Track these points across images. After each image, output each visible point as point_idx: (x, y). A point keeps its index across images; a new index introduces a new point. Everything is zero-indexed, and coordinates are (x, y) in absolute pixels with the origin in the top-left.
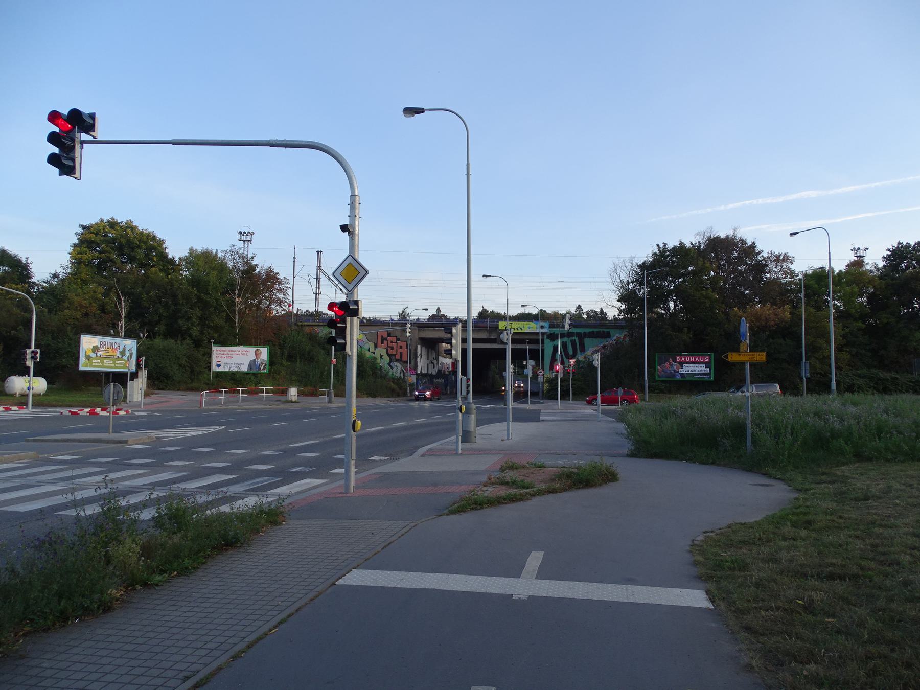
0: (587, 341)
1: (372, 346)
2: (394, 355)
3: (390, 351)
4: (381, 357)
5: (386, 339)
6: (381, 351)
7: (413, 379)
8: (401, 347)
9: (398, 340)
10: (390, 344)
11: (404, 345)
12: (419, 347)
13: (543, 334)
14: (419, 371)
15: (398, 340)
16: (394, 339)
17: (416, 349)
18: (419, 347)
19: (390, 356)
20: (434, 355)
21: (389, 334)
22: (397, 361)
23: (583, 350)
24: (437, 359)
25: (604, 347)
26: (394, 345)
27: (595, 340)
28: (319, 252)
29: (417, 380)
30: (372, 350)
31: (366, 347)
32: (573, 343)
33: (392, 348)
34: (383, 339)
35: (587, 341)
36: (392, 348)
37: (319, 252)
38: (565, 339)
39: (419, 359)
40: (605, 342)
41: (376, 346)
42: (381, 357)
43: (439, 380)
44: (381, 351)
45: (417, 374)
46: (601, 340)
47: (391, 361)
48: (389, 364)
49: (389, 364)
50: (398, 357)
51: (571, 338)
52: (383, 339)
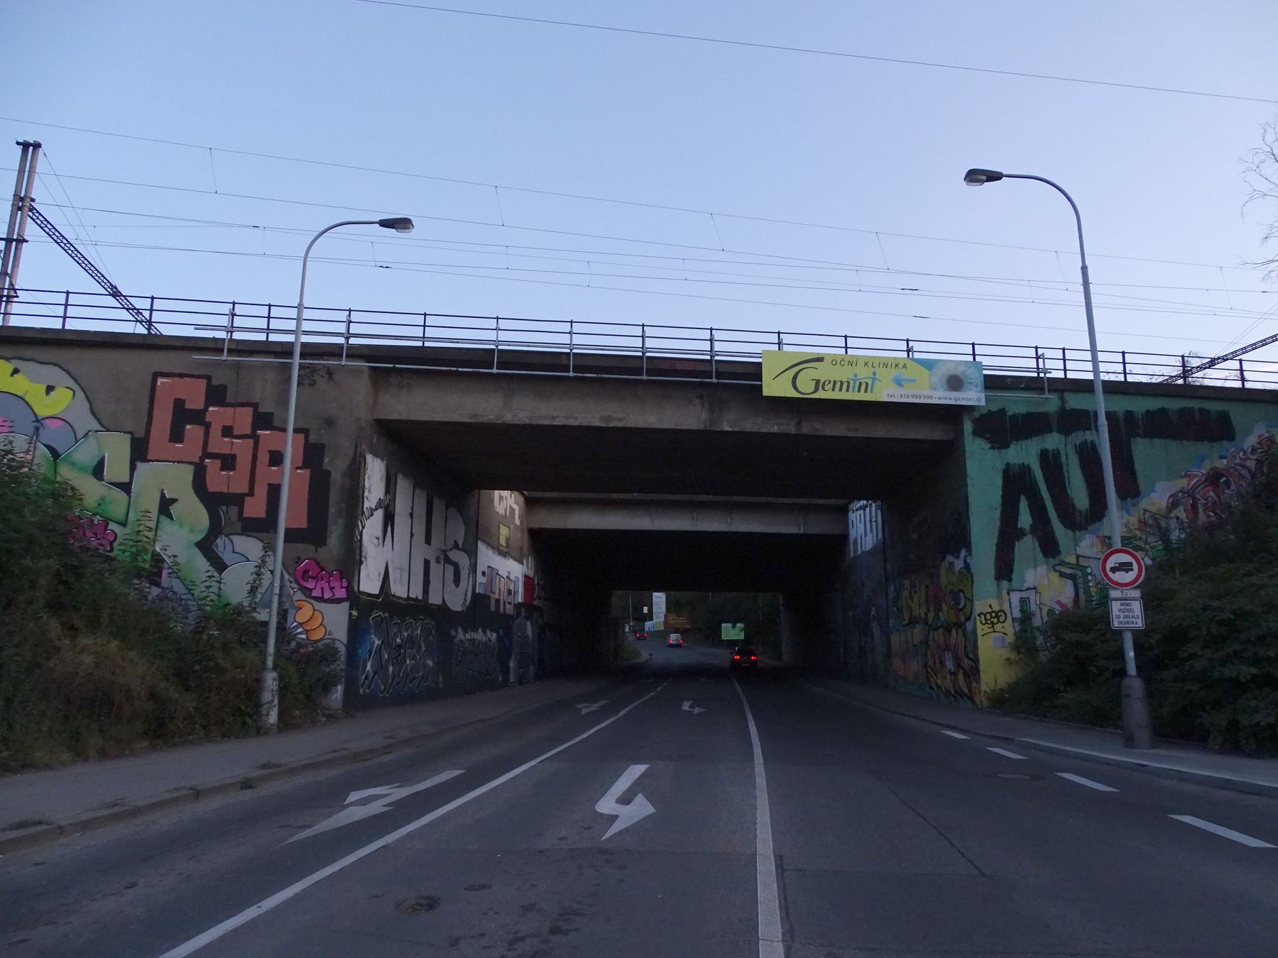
0: (1144, 451)
1: (116, 449)
2: (238, 500)
3: (217, 480)
4: (166, 505)
5: (198, 417)
6: (168, 476)
7: (333, 622)
8: (276, 458)
9: (263, 420)
10: (220, 444)
12: (375, 471)
13: (951, 415)
14: (369, 583)
15: (263, 420)
16: (243, 420)
17: (356, 473)
18: (375, 471)
19: (212, 501)
20: (459, 532)
21: (216, 395)
23: (1130, 489)
24: (473, 554)
25: (1214, 478)
26: (241, 448)
27: (1173, 445)
28: (29, 148)
29: (356, 630)
30: (117, 468)
31: (86, 454)
32: (1089, 457)
33: (228, 462)
34: (183, 416)
35: (1144, 451)
36: (228, 462)
37: (29, 148)
38: (1053, 441)
39: (372, 527)
40: (1215, 457)
41: (140, 451)
42: (166, 505)
43: (479, 636)
44: (168, 476)
45: (355, 598)
46: (1204, 447)
47: (216, 529)
48: (205, 546)
49: (205, 546)
51: (1079, 437)
52: (183, 416)
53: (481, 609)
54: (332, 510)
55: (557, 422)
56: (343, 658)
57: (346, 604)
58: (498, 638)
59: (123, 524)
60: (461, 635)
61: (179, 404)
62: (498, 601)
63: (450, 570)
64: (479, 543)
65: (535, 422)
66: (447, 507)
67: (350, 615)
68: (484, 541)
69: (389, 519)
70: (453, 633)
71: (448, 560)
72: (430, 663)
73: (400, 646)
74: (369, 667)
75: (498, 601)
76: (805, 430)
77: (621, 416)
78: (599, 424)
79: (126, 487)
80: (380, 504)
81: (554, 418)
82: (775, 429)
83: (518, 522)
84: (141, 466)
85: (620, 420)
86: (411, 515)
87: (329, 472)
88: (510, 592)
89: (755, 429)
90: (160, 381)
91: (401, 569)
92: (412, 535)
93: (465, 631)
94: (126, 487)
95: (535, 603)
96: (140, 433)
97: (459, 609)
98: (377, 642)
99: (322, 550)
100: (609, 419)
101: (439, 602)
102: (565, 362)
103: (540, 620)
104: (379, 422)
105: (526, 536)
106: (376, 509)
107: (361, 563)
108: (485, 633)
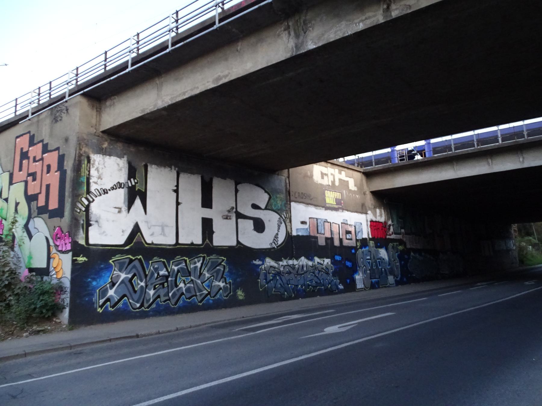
9: (45, 149)
11: (52, 158)
15: (45, 149)
22: (42, 211)
50: (41, 202)
53: (298, 245)
54: (67, 194)
55: (187, 96)
56: (69, 290)
57: (71, 254)
58: (334, 262)
59: (6, 220)
60: (269, 262)
61: (22, 149)
62: (330, 240)
63: (247, 226)
64: (293, 204)
65: (174, 101)
66: (237, 184)
67: (74, 261)
68: (295, 202)
69: (136, 194)
70: (257, 262)
71: (239, 216)
72: (222, 284)
73: (167, 277)
74: (111, 293)
75: (330, 240)
76: (395, 13)
77: (226, 72)
78: (211, 86)
79: (6, 200)
80: (120, 185)
81: (184, 93)
82: (361, 27)
83: (352, 186)
84: (11, 187)
85: (226, 76)
86: (176, 191)
87: (66, 170)
88: (348, 232)
89: (340, 35)
90: (18, 140)
91: (163, 227)
92: (178, 204)
93: (277, 259)
94: (6, 200)
95: (393, 236)
96: (11, 172)
97: (267, 246)
98: (123, 276)
99: (63, 220)
100: (219, 78)
101: (234, 243)
102: (166, 45)
103: (400, 248)
104: (104, 132)
105: (369, 196)
106: (113, 188)
107: (89, 225)
108: (312, 260)
